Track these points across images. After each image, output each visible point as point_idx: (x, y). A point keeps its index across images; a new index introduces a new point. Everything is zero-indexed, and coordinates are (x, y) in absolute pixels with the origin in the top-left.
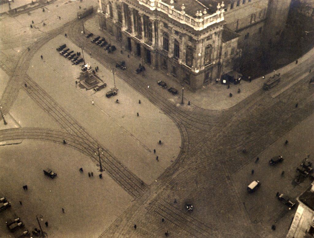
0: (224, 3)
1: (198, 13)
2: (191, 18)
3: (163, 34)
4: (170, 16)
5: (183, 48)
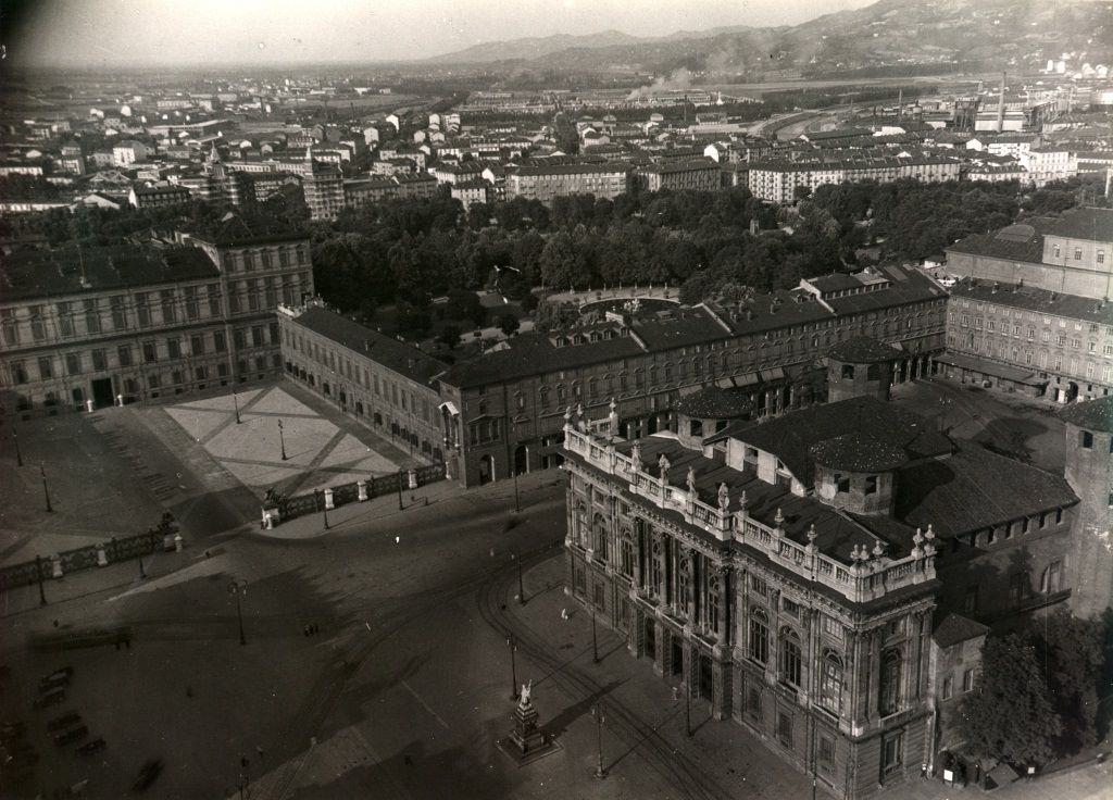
0: (933, 530)
1: (855, 553)
2: (836, 565)
3: (753, 608)
4: (772, 557)
5: (809, 652)
